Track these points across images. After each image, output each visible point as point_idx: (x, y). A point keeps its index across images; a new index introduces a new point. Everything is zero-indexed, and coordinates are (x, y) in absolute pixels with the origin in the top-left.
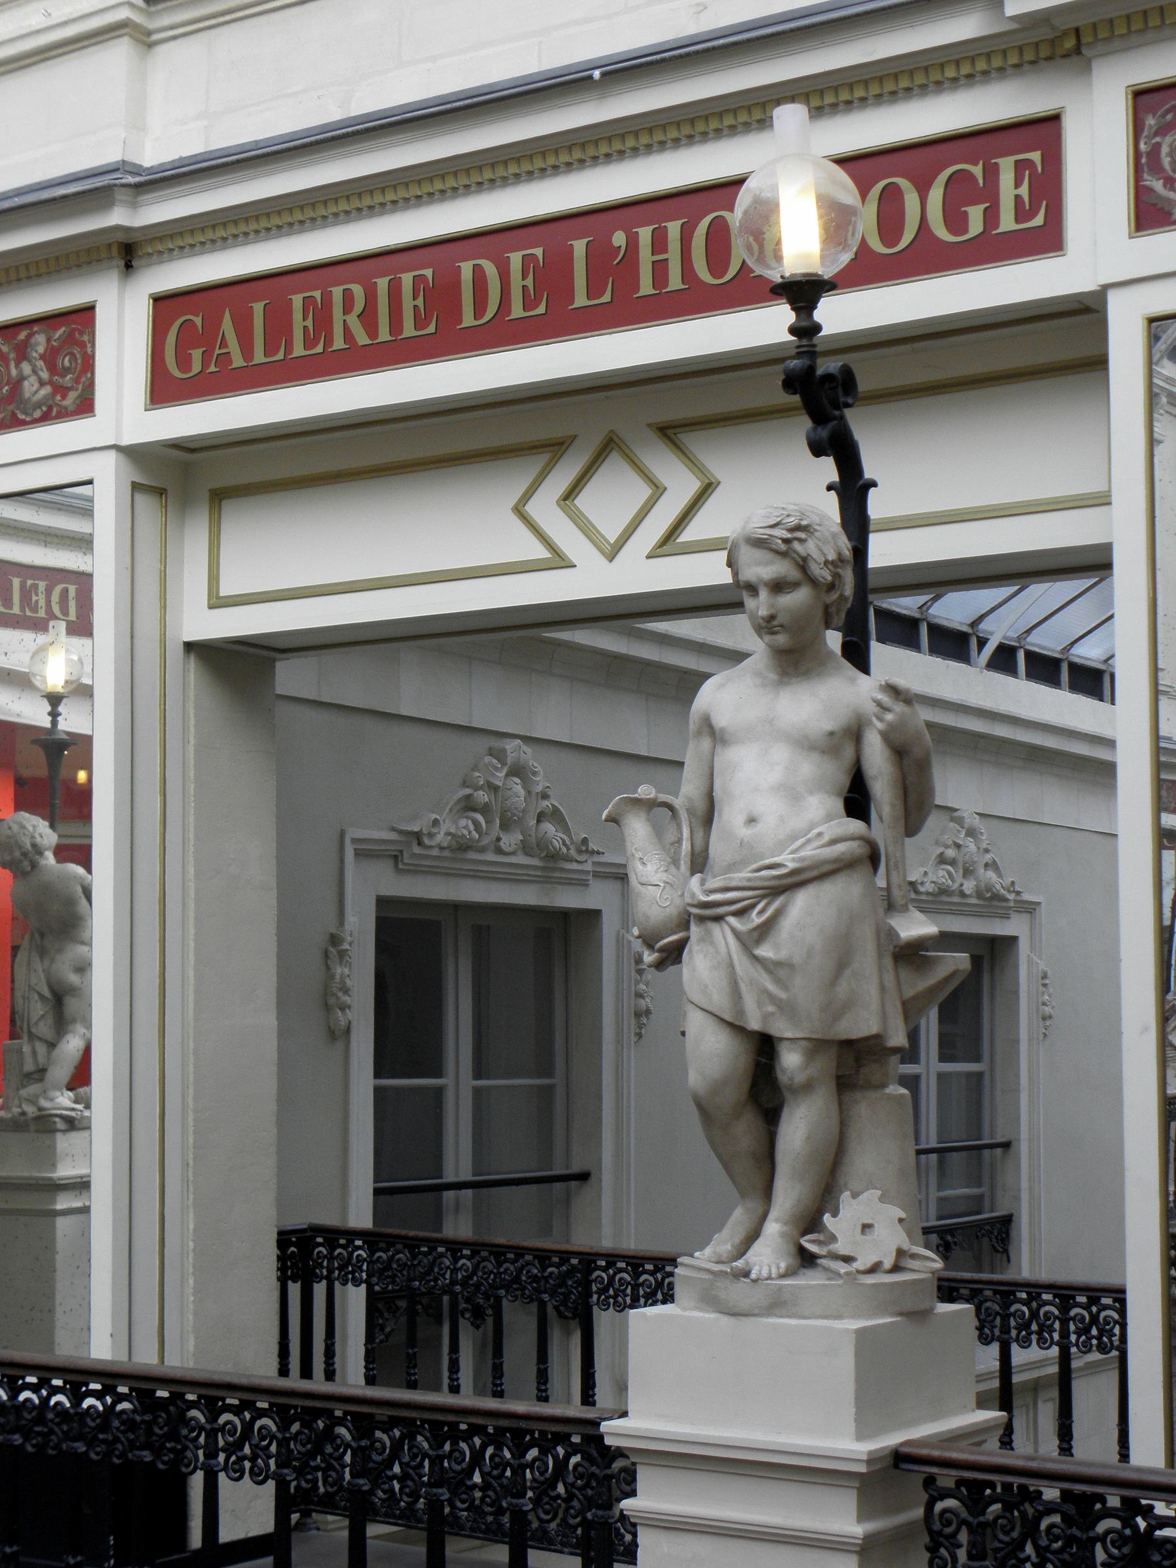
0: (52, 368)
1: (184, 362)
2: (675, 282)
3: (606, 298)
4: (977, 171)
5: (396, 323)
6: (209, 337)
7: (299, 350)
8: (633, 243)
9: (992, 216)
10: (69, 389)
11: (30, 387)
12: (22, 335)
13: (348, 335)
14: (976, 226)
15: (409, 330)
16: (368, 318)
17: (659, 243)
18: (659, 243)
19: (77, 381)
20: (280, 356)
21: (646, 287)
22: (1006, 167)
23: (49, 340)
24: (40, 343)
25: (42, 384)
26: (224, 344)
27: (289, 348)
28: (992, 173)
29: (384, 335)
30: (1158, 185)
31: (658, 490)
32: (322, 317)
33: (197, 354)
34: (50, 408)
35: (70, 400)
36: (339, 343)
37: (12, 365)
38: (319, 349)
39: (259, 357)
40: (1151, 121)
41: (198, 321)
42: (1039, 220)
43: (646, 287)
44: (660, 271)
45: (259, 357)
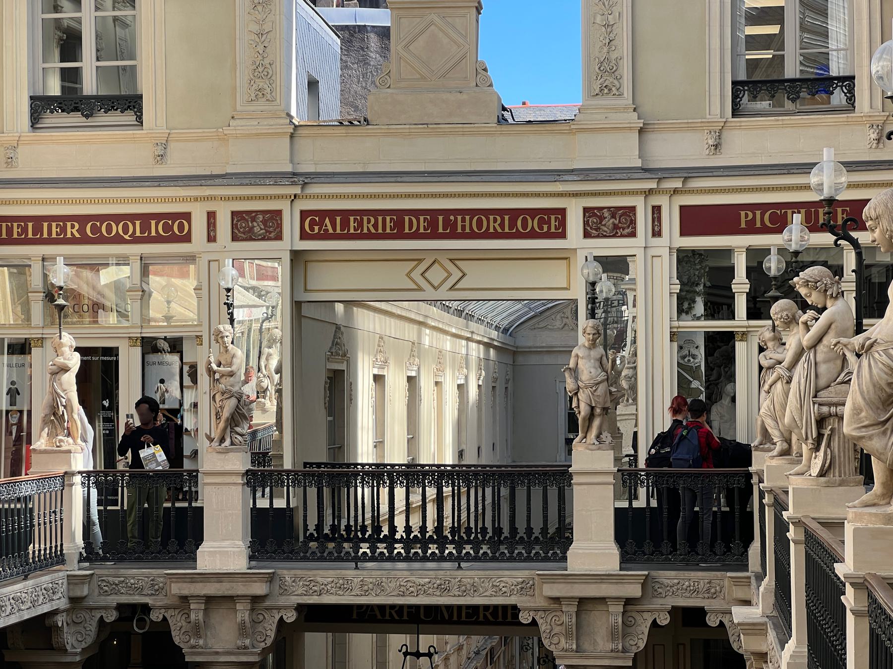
0: (265, 225)
1: (312, 229)
2: (468, 230)
3: (448, 231)
4: (546, 217)
5: (384, 228)
6: (321, 224)
7: (352, 231)
8: (456, 219)
9: (549, 228)
10: (271, 232)
11: (257, 229)
12: (253, 214)
13: (368, 229)
14: (545, 229)
15: (388, 231)
16: (375, 226)
17: (463, 220)
18: (463, 220)
19: (275, 230)
20: (346, 232)
21: (459, 230)
22: (553, 217)
23: (264, 217)
24: (261, 217)
25: (261, 229)
26: (326, 226)
27: (349, 230)
28: (549, 218)
29: (380, 231)
30: (589, 228)
31: (450, 275)
32: (360, 225)
33: (316, 228)
34: (265, 237)
35: (272, 235)
36: (365, 231)
37: (250, 222)
38: (359, 232)
39: (338, 231)
40: (587, 214)
41: (317, 219)
42: (560, 231)
43: (459, 230)
44: (463, 227)
45: (338, 231)
